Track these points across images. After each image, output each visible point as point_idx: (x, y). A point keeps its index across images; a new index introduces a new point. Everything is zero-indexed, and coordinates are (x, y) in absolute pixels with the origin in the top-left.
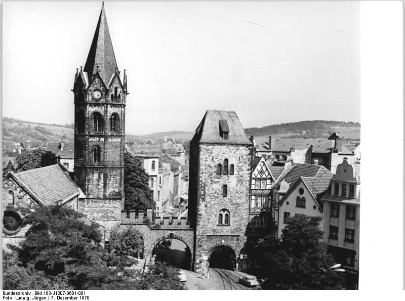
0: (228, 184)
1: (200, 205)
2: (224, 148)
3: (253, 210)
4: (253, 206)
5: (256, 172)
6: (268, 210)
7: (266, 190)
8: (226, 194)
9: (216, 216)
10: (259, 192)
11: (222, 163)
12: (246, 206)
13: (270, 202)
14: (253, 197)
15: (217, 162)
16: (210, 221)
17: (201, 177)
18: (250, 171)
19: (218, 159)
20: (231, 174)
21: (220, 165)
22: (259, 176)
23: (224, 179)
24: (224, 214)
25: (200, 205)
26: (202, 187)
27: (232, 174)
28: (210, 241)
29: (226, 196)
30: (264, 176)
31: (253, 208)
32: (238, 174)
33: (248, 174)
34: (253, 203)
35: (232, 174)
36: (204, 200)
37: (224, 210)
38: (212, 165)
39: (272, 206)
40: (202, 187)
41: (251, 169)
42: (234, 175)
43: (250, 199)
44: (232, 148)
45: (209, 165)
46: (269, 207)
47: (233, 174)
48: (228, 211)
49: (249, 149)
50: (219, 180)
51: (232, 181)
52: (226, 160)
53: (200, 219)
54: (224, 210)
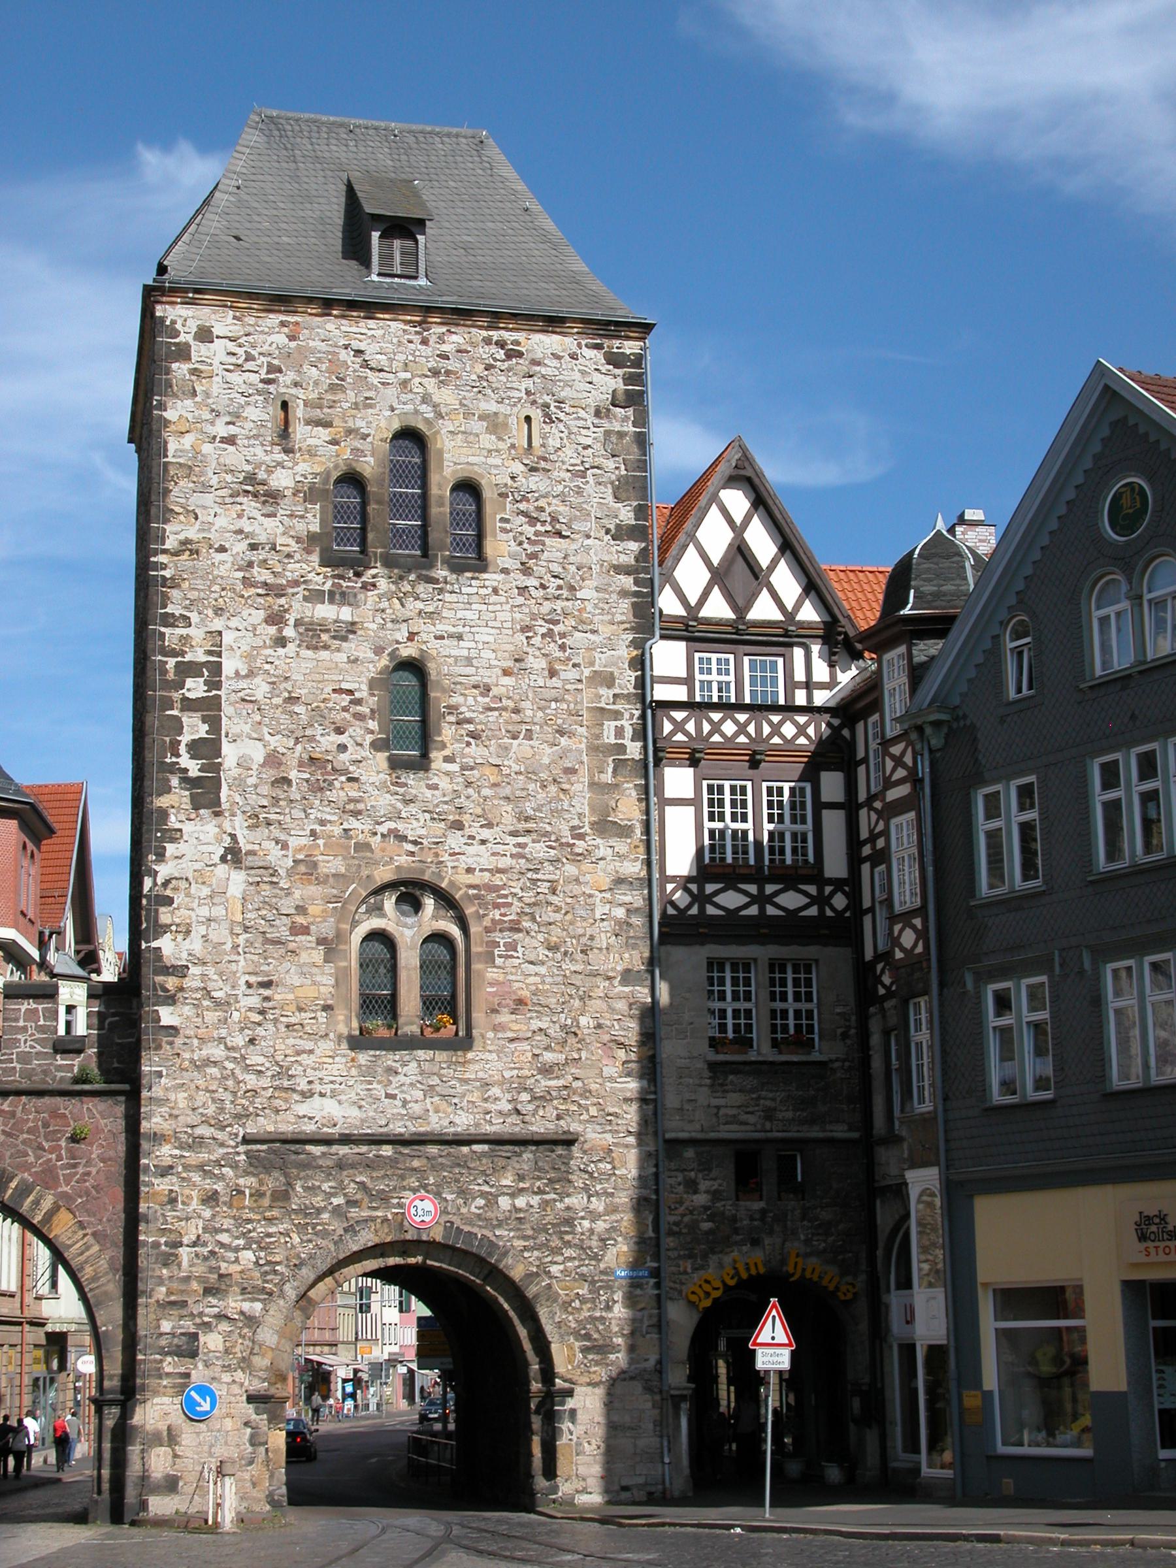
0: (433, 646)
1: (175, 836)
2: (382, 336)
5: (691, 573)
6: (821, 901)
7: (790, 709)
8: (425, 738)
9: (331, 947)
10: (729, 728)
11: (368, 466)
12: (620, 858)
13: (834, 822)
14: (678, 780)
15: (318, 454)
16: (279, 995)
17: (174, 583)
18: (634, 546)
19: (338, 430)
20: (457, 568)
21: (352, 480)
23: (387, 614)
24: (410, 932)
25: (175, 836)
26: (189, 670)
27: (474, 559)
28: (282, 1196)
29: (422, 763)
30: (763, 610)
32: (526, 571)
33: (619, 569)
35: (474, 559)
36: (205, 793)
37: (409, 891)
38: (282, 480)
39: (854, 860)
40: (189, 670)
41: (637, 532)
42: (491, 578)
43: (652, 797)
44: (457, 338)
45: (251, 478)
46: (835, 865)
47: (484, 570)
48: (446, 900)
49: (615, 360)
50: (346, 614)
51: (469, 628)
52: (411, 438)
53: (171, 982)
54: (409, 891)
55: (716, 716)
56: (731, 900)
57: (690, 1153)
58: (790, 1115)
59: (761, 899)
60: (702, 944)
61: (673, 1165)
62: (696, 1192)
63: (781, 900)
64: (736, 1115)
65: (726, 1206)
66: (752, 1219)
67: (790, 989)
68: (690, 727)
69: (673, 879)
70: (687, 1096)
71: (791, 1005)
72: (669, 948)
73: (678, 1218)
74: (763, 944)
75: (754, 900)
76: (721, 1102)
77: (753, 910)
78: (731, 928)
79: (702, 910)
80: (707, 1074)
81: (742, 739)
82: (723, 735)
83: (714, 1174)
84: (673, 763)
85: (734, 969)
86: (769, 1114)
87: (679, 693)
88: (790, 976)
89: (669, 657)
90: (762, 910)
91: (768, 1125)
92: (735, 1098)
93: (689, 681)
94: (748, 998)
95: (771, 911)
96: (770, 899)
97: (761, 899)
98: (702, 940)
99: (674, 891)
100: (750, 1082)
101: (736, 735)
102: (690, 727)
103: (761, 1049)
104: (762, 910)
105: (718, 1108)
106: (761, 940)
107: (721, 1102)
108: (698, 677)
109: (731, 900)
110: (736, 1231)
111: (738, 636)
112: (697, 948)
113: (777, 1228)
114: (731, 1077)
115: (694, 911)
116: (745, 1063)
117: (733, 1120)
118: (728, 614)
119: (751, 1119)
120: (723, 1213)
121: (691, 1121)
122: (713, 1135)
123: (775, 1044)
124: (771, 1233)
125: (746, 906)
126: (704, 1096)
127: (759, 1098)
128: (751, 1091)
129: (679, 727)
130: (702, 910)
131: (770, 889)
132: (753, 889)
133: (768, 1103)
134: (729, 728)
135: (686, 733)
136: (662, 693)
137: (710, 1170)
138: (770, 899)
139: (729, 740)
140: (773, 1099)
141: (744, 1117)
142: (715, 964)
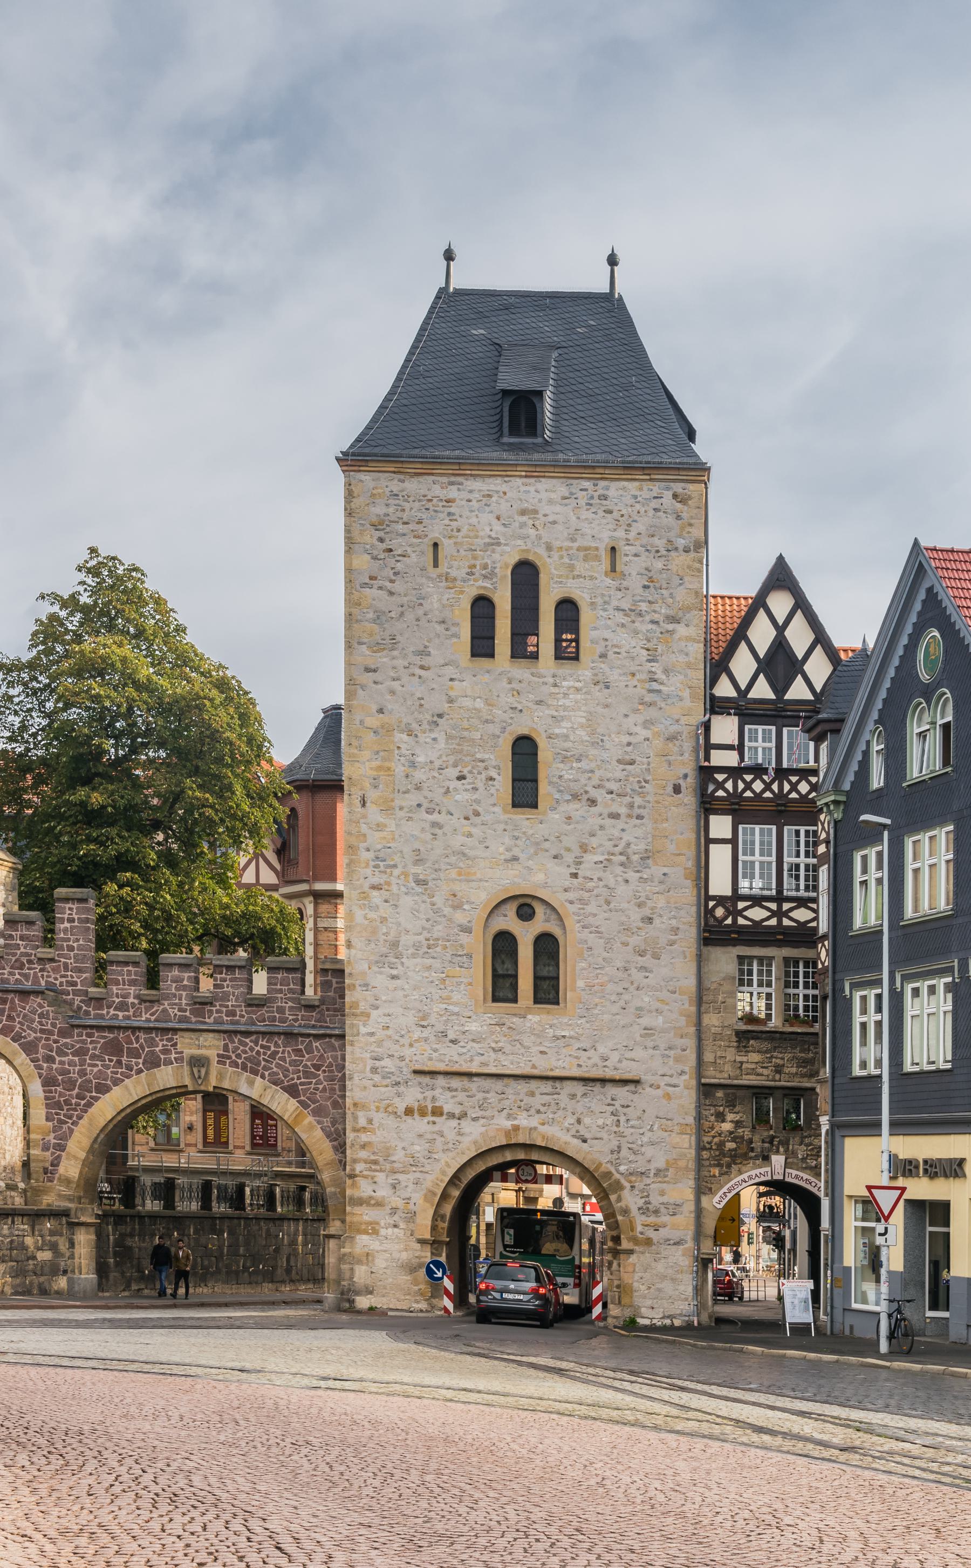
3: (720, 912)
4: (720, 885)
10: (758, 786)
14: (721, 826)
22: (763, 690)
24: (526, 935)
31: (721, 900)
34: (720, 857)
55: (748, 778)
56: (757, 914)
57: (720, 1094)
58: (794, 1070)
59: (779, 914)
60: (734, 945)
61: (707, 1102)
62: (723, 1121)
63: (796, 914)
64: (755, 1068)
65: (746, 1133)
66: (763, 1142)
67: (801, 980)
68: (729, 785)
69: (714, 898)
70: (719, 1054)
71: (801, 991)
72: (710, 948)
73: (709, 1139)
74: (779, 947)
75: (774, 914)
76: (745, 1059)
77: (773, 922)
78: (757, 935)
79: (734, 921)
80: (734, 1039)
81: (768, 794)
82: (753, 791)
83: (737, 1109)
84: (717, 812)
85: (761, 964)
86: (779, 1070)
87: (729, 759)
88: (801, 970)
89: (725, 729)
90: (780, 921)
91: (777, 1077)
92: (755, 1057)
93: (740, 748)
94: (769, 984)
95: (786, 922)
96: (786, 914)
97: (779, 914)
98: (734, 943)
99: (715, 907)
100: (766, 1045)
101: (763, 791)
102: (729, 785)
103: (775, 1023)
104: (780, 921)
105: (742, 1063)
106: (780, 944)
107: (745, 1059)
108: (747, 743)
109: (757, 914)
110: (752, 1150)
111: (777, 713)
112: (730, 949)
113: (781, 1149)
114: (752, 1042)
115: (729, 921)
116: (762, 1032)
117: (753, 1072)
118: (771, 695)
119: (765, 1072)
120: (743, 1137)
121: (721, 1072)
122: (736, 1082)
123: (786, 1020)
124: (777, 1152)
125: (768, 919)
126: (731, 1054)
127: (772, 1057)
128: (766, 1052)
129: (720, 786)
130: (734, 921)
131: (786, 906)
132: (773, 906)
133: (778, 1061)
134: (758, 786)
135: (726, 791)
136: (720, 758)
137: (734, 1106)
138: (786, 914)
139: (758, 796)
140: (783, 1059)
141: (760, 1070)
142: (741, 959)
